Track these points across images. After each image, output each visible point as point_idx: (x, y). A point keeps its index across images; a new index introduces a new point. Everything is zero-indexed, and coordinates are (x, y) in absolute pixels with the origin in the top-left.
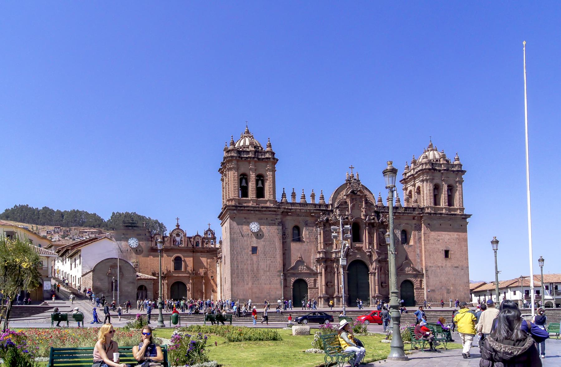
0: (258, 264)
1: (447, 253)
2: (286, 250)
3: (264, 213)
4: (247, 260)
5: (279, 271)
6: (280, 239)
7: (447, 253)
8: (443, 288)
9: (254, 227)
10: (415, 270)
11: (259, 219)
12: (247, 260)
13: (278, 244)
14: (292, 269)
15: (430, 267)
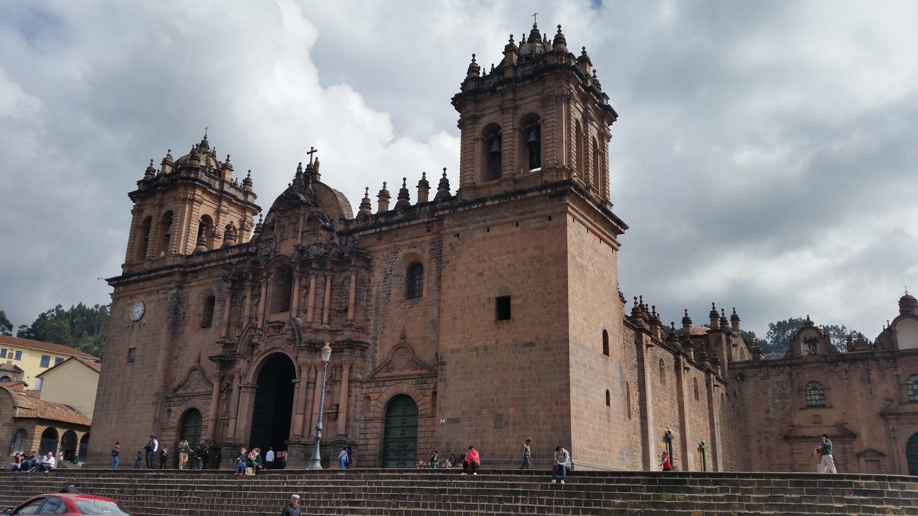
0: (131, 383)
1: (504, 308)
2: (180, 348)
3: (156, 281)
4: (119, 375)
5: (156, 395)
6: (169, 328)
7: (504, 308)
8: (485, 412)
9: (137, 310)
10: (417, 363)
11: (149, 293)
12: (119, 375)
13: (164, 339)
14: (180, 386)
15: (453, 351)
